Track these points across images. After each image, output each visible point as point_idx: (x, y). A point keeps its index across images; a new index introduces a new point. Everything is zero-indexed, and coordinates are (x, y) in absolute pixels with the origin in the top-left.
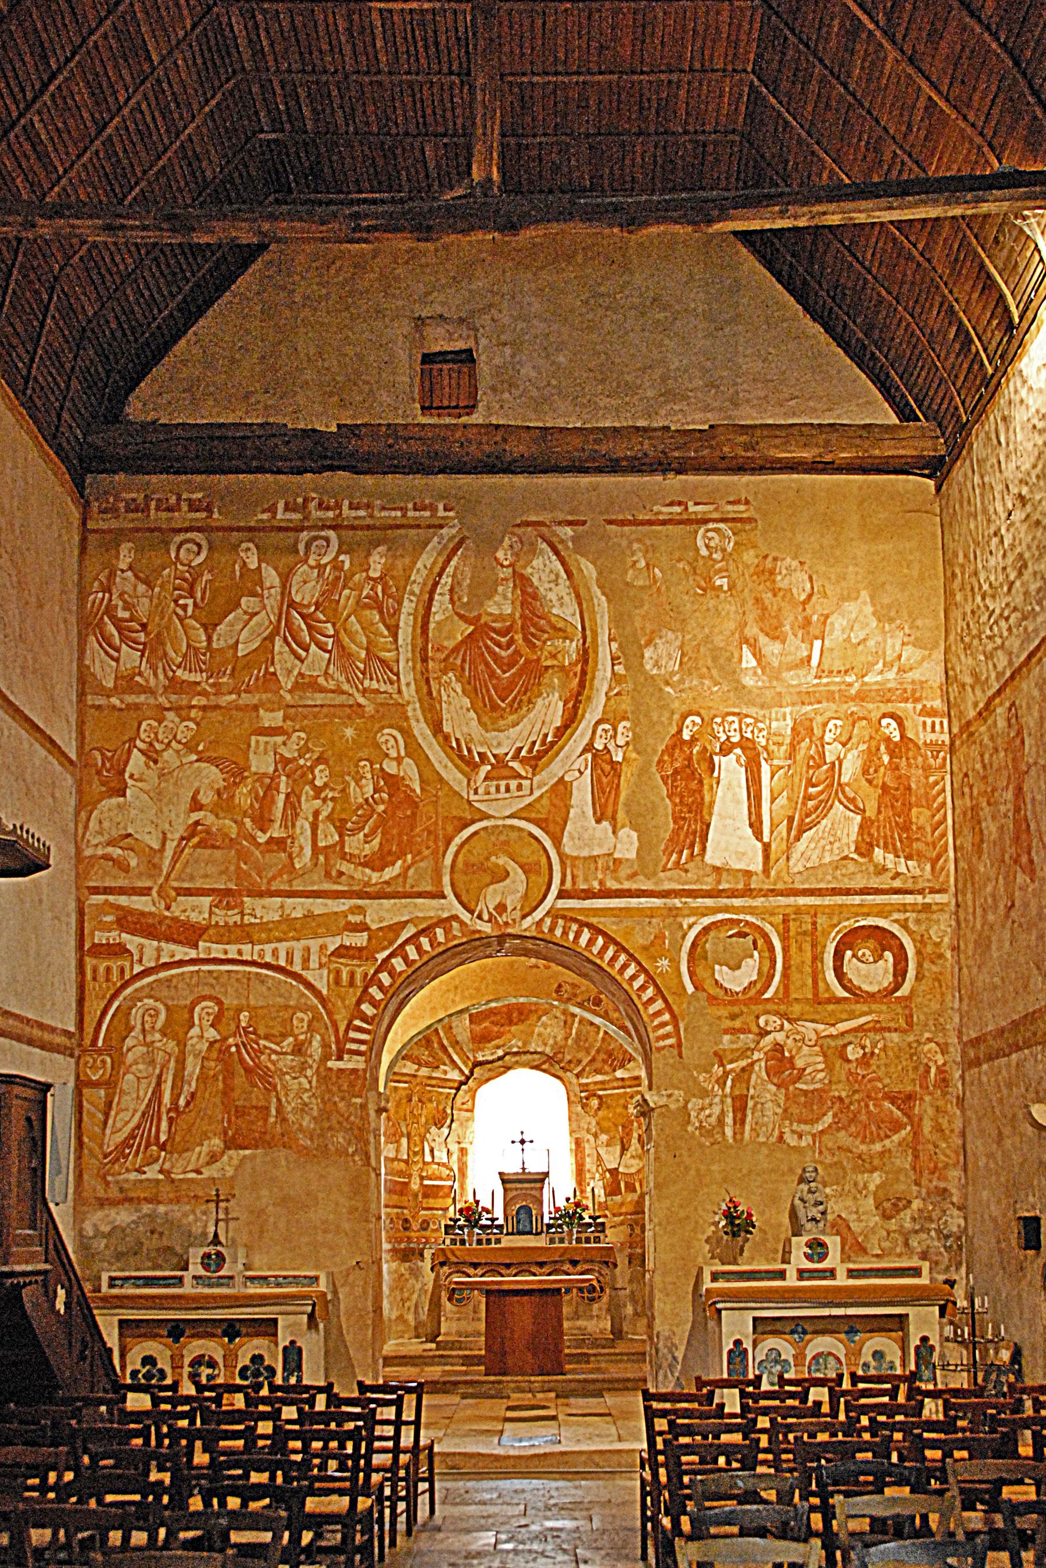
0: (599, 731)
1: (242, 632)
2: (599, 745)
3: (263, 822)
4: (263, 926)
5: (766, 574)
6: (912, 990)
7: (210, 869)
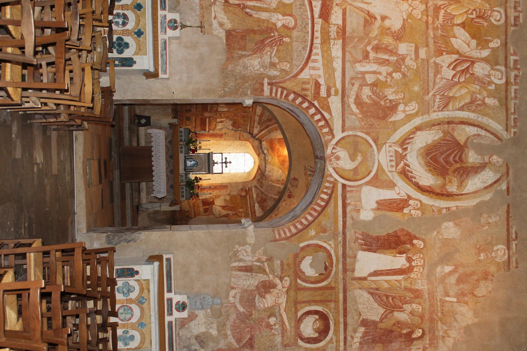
0: (417, 202)
1: (461, 40)
2: (411, 202)
3: (377, 49)
4: (329, 49)
5: (486, 276)
6: (300, 346)
7: (354, 23)
